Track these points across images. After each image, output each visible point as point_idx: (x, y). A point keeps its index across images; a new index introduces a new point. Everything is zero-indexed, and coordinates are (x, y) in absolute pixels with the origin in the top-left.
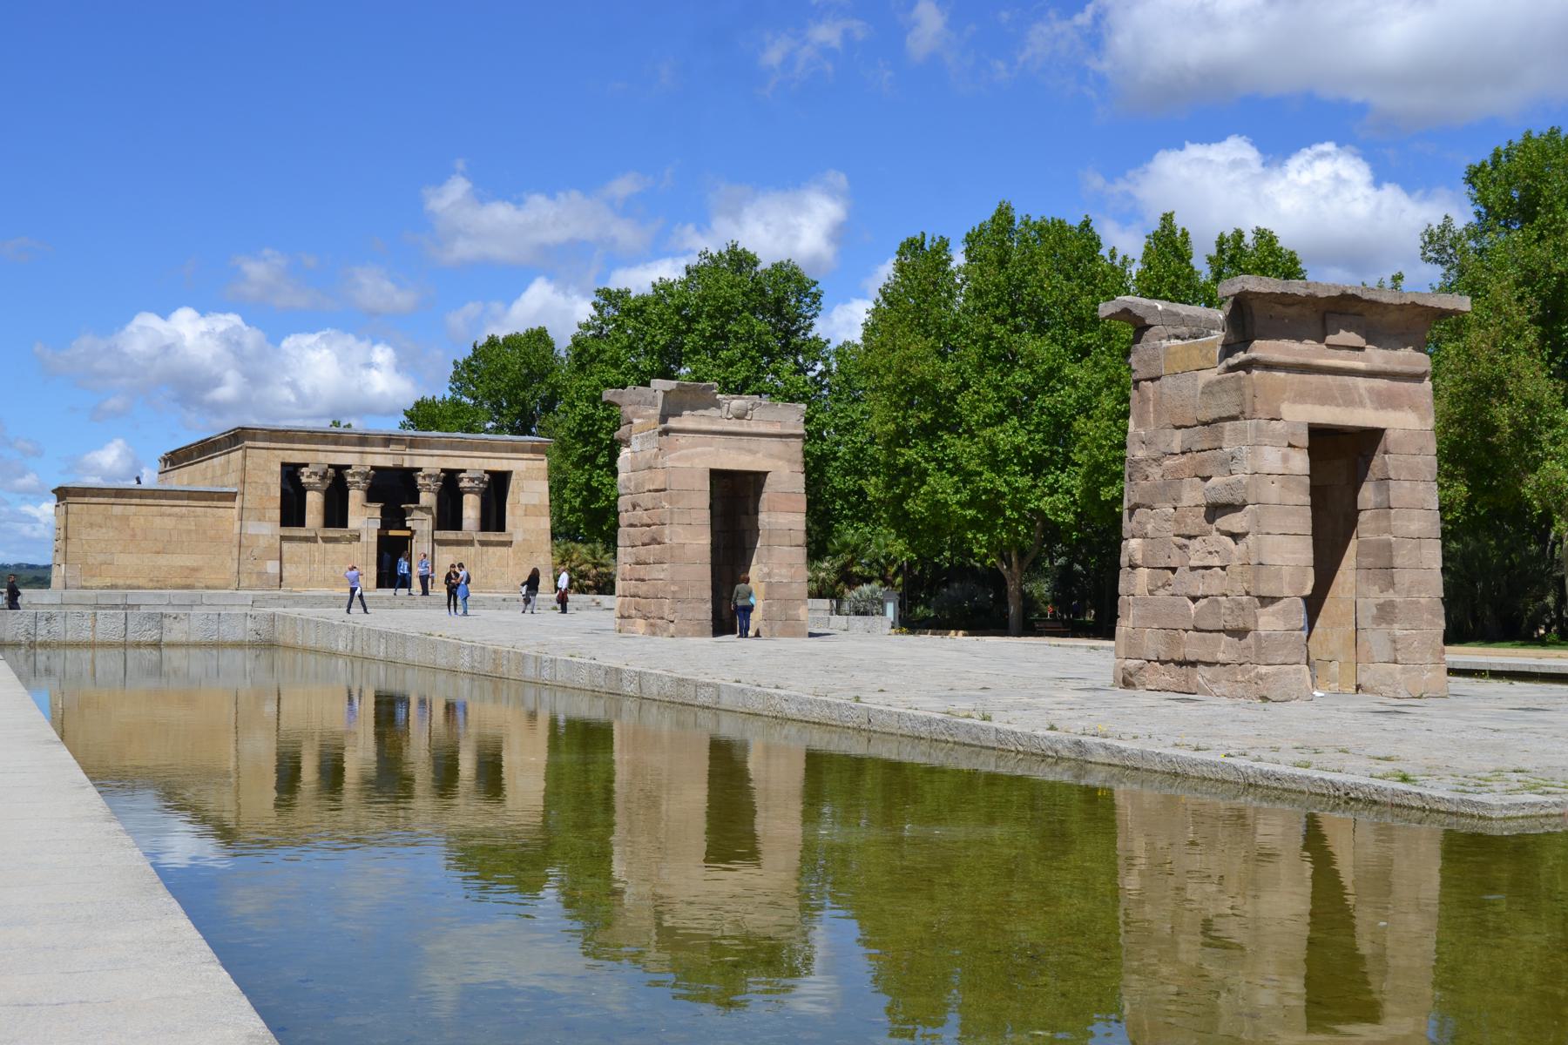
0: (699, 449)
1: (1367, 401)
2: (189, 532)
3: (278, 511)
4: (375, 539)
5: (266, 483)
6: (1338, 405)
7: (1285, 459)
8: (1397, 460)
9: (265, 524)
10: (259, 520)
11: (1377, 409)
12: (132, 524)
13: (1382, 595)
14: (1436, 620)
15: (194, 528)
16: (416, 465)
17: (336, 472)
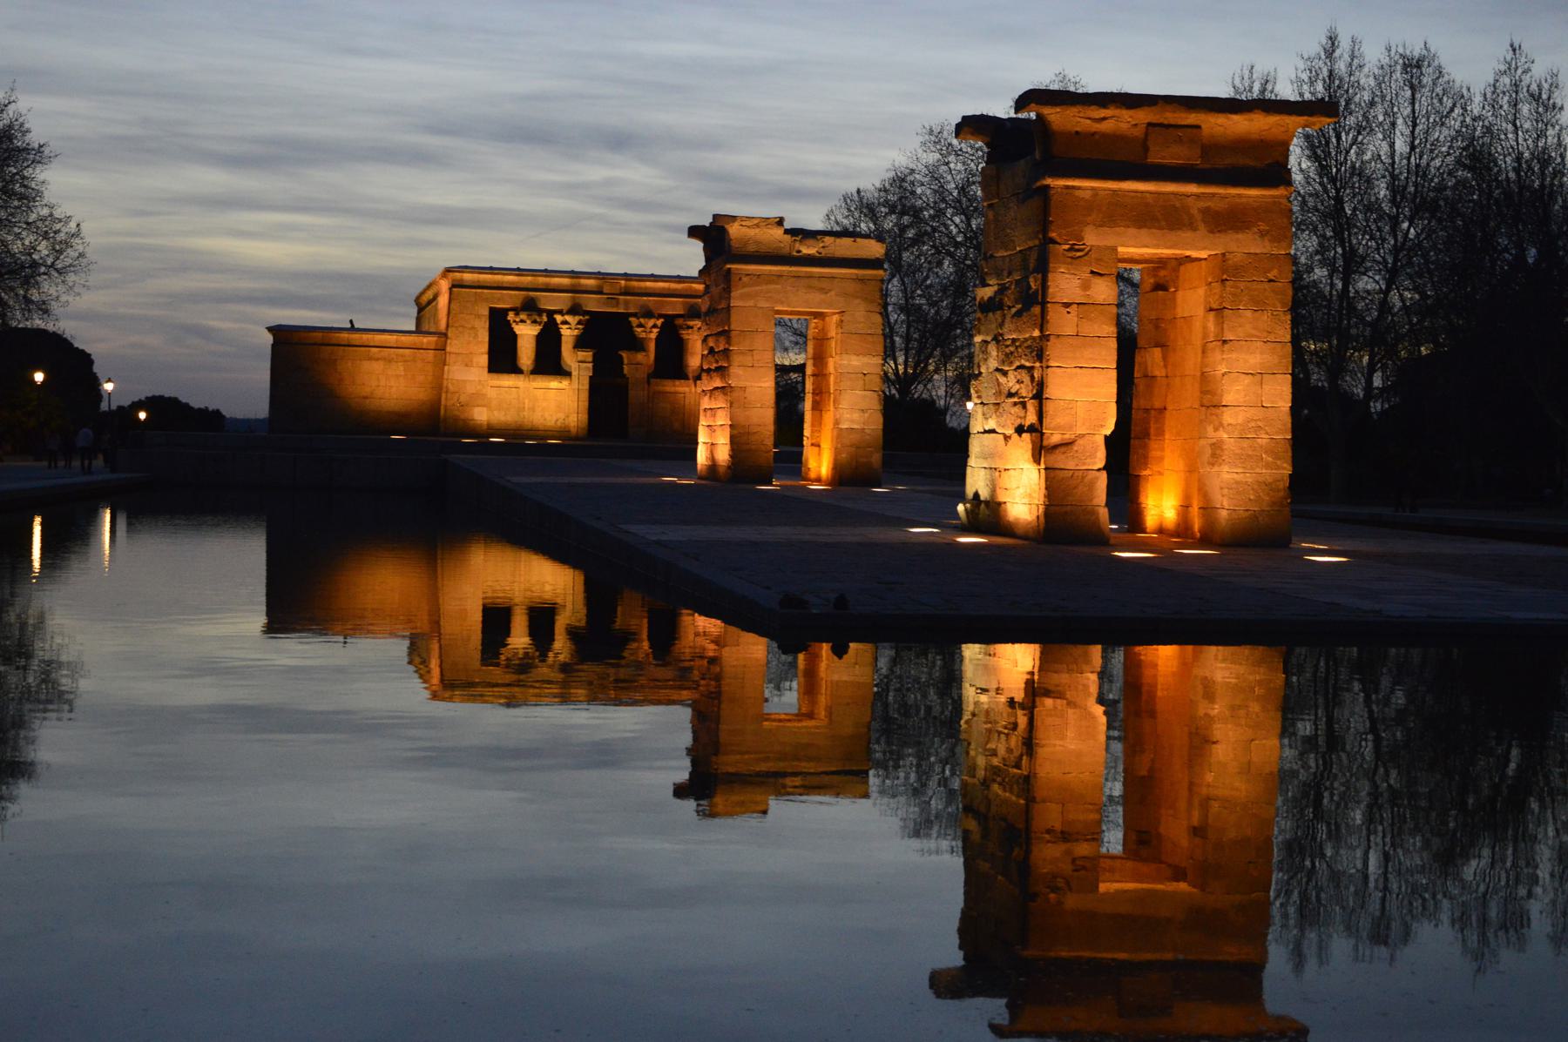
0: (764, 287)
1: (1202, 227)
2: (398, 376)
3: (485, 358)
4: (587, 387)
5: (473, 328)
6: (1160, 228)
7: (1086, 286)
8: (1237, 287)
9: (474, 370)
10: (467, 365)
11: (1212, 232)
13: (1217, 433)
14: (1279, 462)
15: (403, 373)
16: (632, 310)
17: (547, 316)
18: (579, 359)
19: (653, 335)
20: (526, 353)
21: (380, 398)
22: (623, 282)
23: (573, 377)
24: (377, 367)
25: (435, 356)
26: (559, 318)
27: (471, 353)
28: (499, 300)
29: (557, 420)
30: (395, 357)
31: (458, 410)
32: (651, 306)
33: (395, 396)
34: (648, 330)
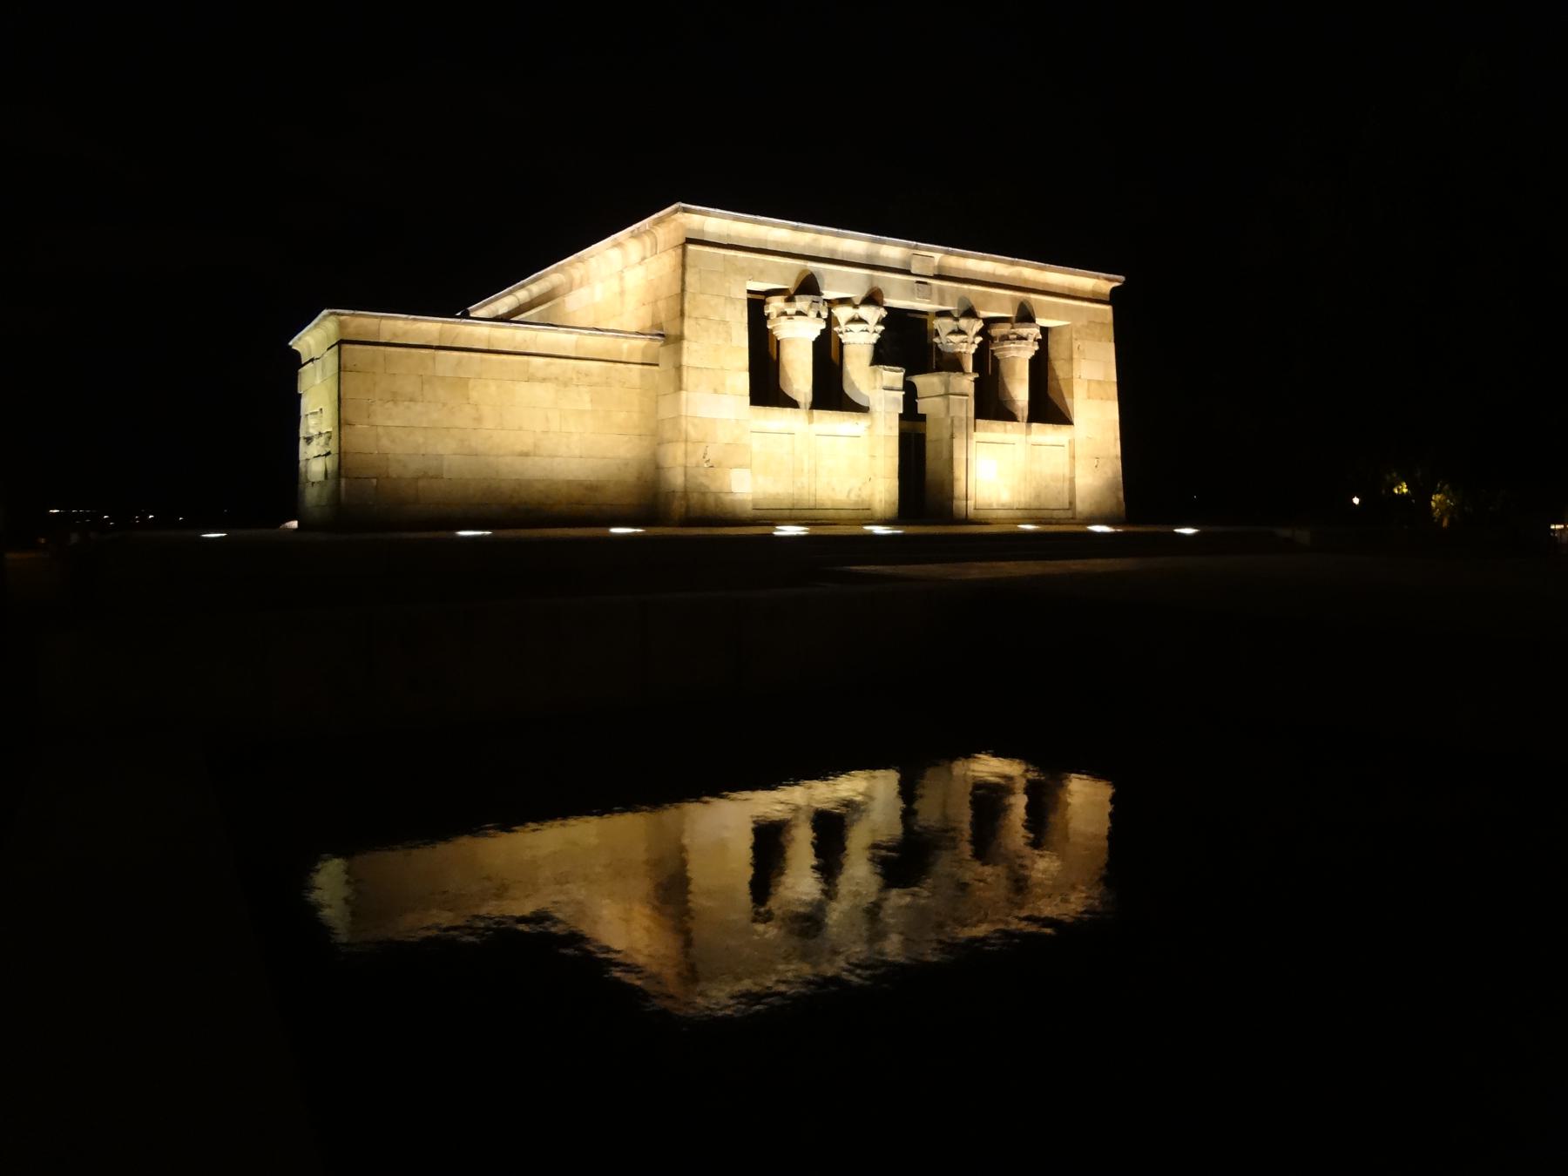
5: (724, 322)
10: (716, 391)
12: (474, 395)
18: (886, 383)
19: (973, 351)
20: (799, 375)
21: (552, 456)
22: (937, 257)
23: (876, 415)
24: (543, 394)
25: (642, 376)
26: (843, 313)
27: (722, 369)
28: (762, 272)
29: (849, 492)
30: (574, 377)
31: (706, 476)
32: (973, 303)
33: (577, 452)
34: (971, 340)
